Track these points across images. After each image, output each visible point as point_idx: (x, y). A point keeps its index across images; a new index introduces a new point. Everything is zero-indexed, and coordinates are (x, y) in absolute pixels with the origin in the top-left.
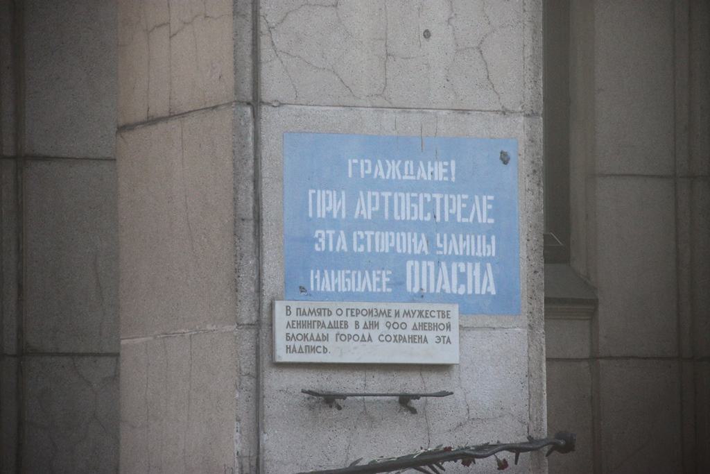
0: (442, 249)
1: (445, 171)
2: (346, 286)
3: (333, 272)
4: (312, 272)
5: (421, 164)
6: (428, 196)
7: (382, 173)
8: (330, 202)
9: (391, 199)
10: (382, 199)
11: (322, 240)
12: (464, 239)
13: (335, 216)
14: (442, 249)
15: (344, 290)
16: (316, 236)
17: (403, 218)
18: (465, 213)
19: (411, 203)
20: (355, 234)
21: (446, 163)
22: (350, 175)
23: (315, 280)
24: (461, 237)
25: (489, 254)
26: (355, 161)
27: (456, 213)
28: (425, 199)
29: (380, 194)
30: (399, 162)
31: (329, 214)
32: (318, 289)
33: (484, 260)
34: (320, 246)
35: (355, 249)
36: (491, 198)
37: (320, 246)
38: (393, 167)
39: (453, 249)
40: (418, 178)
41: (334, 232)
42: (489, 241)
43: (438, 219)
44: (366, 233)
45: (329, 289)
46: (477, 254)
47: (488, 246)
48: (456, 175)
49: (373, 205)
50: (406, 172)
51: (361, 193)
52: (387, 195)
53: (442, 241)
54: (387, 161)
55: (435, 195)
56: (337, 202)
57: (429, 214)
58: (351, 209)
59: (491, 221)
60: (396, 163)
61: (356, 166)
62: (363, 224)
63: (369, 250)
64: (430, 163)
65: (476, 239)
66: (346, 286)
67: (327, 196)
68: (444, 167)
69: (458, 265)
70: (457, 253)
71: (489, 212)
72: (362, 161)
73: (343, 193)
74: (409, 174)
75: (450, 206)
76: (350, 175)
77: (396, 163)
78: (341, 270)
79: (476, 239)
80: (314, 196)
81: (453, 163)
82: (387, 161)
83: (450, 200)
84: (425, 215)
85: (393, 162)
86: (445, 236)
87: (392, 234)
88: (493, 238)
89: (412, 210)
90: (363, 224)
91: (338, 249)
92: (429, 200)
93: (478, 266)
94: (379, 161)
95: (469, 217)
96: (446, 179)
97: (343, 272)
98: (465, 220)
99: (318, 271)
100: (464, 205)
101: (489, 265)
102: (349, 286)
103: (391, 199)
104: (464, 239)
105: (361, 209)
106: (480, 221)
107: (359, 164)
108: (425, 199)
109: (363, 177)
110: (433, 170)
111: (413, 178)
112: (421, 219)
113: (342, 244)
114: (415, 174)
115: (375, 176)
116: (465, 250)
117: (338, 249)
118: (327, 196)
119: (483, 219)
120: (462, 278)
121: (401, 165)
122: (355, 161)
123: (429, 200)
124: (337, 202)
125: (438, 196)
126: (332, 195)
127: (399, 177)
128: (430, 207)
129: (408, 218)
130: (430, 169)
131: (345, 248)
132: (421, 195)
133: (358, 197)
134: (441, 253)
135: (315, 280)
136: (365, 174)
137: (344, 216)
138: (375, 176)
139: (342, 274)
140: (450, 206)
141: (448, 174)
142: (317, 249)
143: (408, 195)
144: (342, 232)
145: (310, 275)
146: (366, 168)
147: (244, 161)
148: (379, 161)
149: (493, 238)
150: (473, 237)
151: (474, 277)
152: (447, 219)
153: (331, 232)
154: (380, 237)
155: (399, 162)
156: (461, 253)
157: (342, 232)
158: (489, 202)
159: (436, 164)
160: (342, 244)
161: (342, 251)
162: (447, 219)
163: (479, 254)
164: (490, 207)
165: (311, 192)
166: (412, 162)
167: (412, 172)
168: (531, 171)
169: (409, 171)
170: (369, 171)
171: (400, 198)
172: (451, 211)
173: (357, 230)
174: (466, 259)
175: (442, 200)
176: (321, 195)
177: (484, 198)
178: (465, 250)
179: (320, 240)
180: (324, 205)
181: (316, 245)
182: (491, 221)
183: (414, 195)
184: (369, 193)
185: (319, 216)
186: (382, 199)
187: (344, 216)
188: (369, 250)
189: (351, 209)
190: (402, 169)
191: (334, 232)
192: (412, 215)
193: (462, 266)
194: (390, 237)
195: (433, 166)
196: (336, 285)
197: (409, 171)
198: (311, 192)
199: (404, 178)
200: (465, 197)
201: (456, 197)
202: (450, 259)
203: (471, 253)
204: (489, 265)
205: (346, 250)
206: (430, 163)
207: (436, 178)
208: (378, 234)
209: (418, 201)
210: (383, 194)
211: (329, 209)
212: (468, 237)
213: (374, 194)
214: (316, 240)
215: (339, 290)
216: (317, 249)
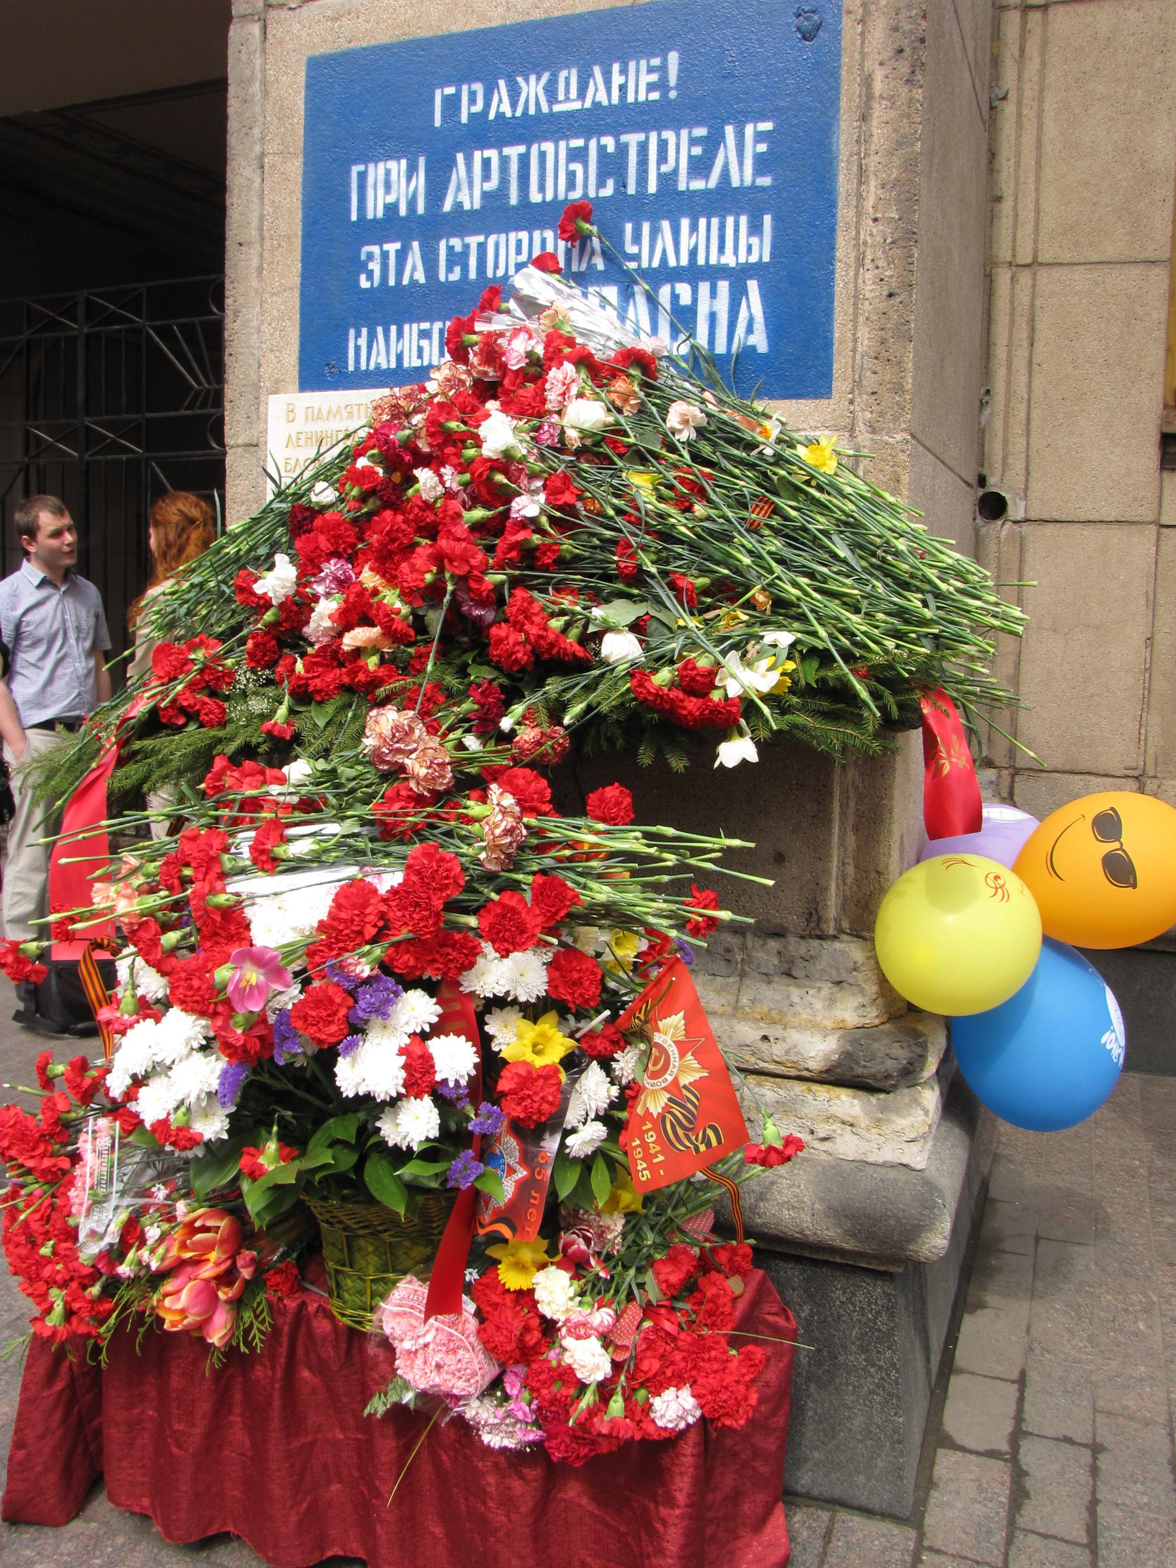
0: (636, 258)
1: (654, 77)
2: (420, 356)
3: (393, 328)
4: (352, 332)
5: (597, 71)
6: (609, 142)
7: (506, 109)
8: (394, 187)
9: (524, 160)
10: (504, 161)
11: (375, 266)
12: (694, 228)
13: (403, 211)
14: (636, 258)
15: (417, 363)
16: (363, 257)
17: (549, 197)
18: (700, 167)
19: (567, 163)
20: (443, 245)
21: (656, 62)
22: (438, 123)
23: (358, 348)
24: (685, 223)
25: (754, 259)
26: (450, 90)
27: (676, 171)
28: (602, 149)
29: (500, 153)
30: (546, 77)
31: (392, 209)
32: (363, 367)
33: (738, 277)
34: (370, 276)
35: (442, 278)
36: (766, 126)
37: (370, 276)
38: (533, 89)
39: (664, 251)
40: (588, 104)
41: (398, 246)
42: (755, 229)
43: (631, 190)
44: (468, 240)
45: (384, 366)
46: (723, 261)
47: (755, 241)
48: (678, 87)
49: (486, 177)
50: (561, 97)
51: (460, 157)
52: (514, 152)
53: (637, 239)
54: (520, 80)
55: (624, 138)
56: (409, 179)
57: (610, 183)
58: (436, 190)
59: (765, 181)
60: (538, 79)
61: (452, 104)
62: (463, 222)
63: (473, 275)
64: (616, 67)
65: (722, 228)
66: (420, 356)
67: (388, 173)
68: (650, 70)
69: (673, 288)
70: (672, 263)
71: (759, 160)
72: (465, 88)
73: (422, 161)
74: (567, 99)
75: (662, 158)
76: (438, 123)
77: (538, 79)
78: (411, 322)
79: (722, 228)
80: (362, 176)
81: (673, 58)
82: (520, 80)
83: (663, 146)
84: (601, 184)
85: (533, 78)
86: (646, 227)
87: (524, 235)
88: (767, 219)
89: (571, 176)
90: (463, 222)
91: (405, 282)
92: (611, 149)
93: (723, 286)
94: (502, 83)
95: (707, 177)
96: (655, 96)
97: (415, 326)
98: (698, 185)
99: (364, 331)
100: (697, 151)
101: (753, 286)
102: (426, 355)
103: (524, 160)
104: (694, 228)
105: (458, 189)
106: (735, 183)
107: (457, 97)
108: (602, 149)
109: (464, 119)
110: (622, 80)
111: (577, 106)
112: (592, 194)
113: (414, 269)
114: (582, 95)
115: (492, 116)
116: (693, 253)
117: (405, 282)
118: (388, 173)
119: (743, 175)
120: (684, 318)
121: (549, 81)
122: (450, 90)
123: (611, 149)
124: (409, 179)
125: (633, 139)
126: (397, 168)
127: (545, 109)
128: (612, 166)
129: (561, 196)
130: (617, 80)
131: (420, 277)
132: (593, 144)
133: (452, 163)
134: (632, 265)
135: (358, 348)
136: (471, 116)
137: (421, 209)
138: (492, 116)
139: (412, 330)
140: (662, 158)
141: (661, 85)
142: (364, 284)
143: (562, 144)
144: (416, 245)
145: (347, 340)
146: (472, 101)
147: (244, 130)
148: (502, 83)
149: (767, 219)
150: (715, 222)
151: (713, 317)
152: (652, 188)
153: (392, 247)
154: (497, 245)
155: (546, 77)
156: (684, 261)
157: (416, 245)
158: (760, 137)
159: (632, 65)
160: (414, 269)
161: (413, 283)
162: (652, 188)
163: (729, 260)
164: (762, 148)
165: (356, 169)
166: (574, 73)
167: (573, 93)
168: (888, 54)
169: (567, 91)
170: (478, 107)
171: (542, 156)
172: (664, 169)
173: (451, 235)
174: (694, 274)
175: (643, 148)
176: (376, 172)
177: (749, 130)
178: (693, 253)
179: (371, 266)
180: (381, 191)
181: (363, 277)
182: (765, 181)
183: (578, 143)
184: (477, 155)
185: (370, 216)
186: (504, 161)
187: (421, 209)
188: (473, 275)
189: (436, 190)
190: (551, 92)
191: (398, 246)
192: (571, 185)
193: (684, 291)
194: (519, 243)
195: (624, 71)
196: (400, 357)
197: (567, 91)
198: (356, 169)
199: (557, 108)
200: (701, 132)
201: (678, 136)
202: (665, 274)
203: (707, 260)
204: (753, 286)
205: (422, 280)
206: (616, 67)
207: (631, 98)
208: (492, 239)
209: (587, 155)
210: (506, 151)
211: (391, 199)
212: (702, 222)
213: (488, 153)
214: (362, 267)
215: (406, 365)
216: (364, 284)
